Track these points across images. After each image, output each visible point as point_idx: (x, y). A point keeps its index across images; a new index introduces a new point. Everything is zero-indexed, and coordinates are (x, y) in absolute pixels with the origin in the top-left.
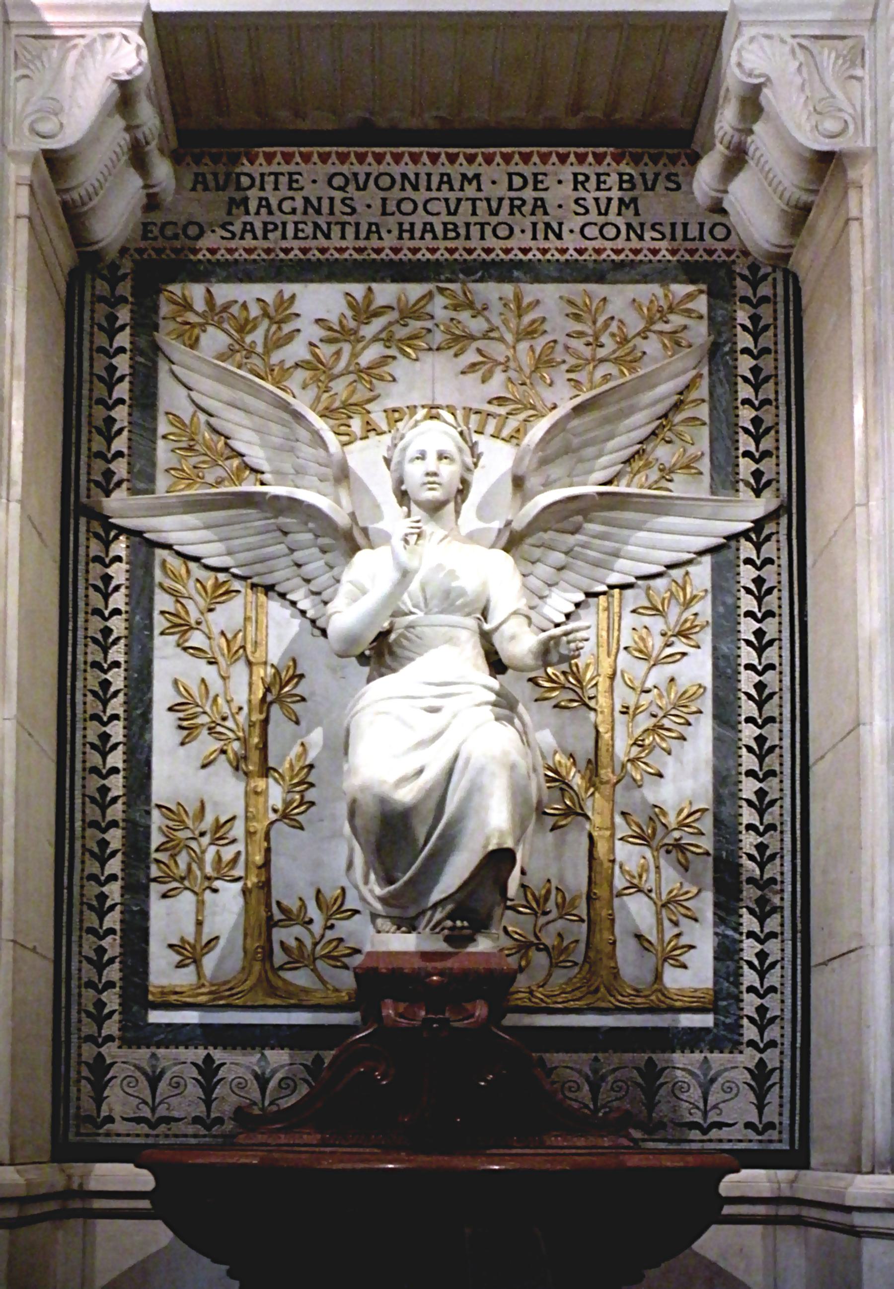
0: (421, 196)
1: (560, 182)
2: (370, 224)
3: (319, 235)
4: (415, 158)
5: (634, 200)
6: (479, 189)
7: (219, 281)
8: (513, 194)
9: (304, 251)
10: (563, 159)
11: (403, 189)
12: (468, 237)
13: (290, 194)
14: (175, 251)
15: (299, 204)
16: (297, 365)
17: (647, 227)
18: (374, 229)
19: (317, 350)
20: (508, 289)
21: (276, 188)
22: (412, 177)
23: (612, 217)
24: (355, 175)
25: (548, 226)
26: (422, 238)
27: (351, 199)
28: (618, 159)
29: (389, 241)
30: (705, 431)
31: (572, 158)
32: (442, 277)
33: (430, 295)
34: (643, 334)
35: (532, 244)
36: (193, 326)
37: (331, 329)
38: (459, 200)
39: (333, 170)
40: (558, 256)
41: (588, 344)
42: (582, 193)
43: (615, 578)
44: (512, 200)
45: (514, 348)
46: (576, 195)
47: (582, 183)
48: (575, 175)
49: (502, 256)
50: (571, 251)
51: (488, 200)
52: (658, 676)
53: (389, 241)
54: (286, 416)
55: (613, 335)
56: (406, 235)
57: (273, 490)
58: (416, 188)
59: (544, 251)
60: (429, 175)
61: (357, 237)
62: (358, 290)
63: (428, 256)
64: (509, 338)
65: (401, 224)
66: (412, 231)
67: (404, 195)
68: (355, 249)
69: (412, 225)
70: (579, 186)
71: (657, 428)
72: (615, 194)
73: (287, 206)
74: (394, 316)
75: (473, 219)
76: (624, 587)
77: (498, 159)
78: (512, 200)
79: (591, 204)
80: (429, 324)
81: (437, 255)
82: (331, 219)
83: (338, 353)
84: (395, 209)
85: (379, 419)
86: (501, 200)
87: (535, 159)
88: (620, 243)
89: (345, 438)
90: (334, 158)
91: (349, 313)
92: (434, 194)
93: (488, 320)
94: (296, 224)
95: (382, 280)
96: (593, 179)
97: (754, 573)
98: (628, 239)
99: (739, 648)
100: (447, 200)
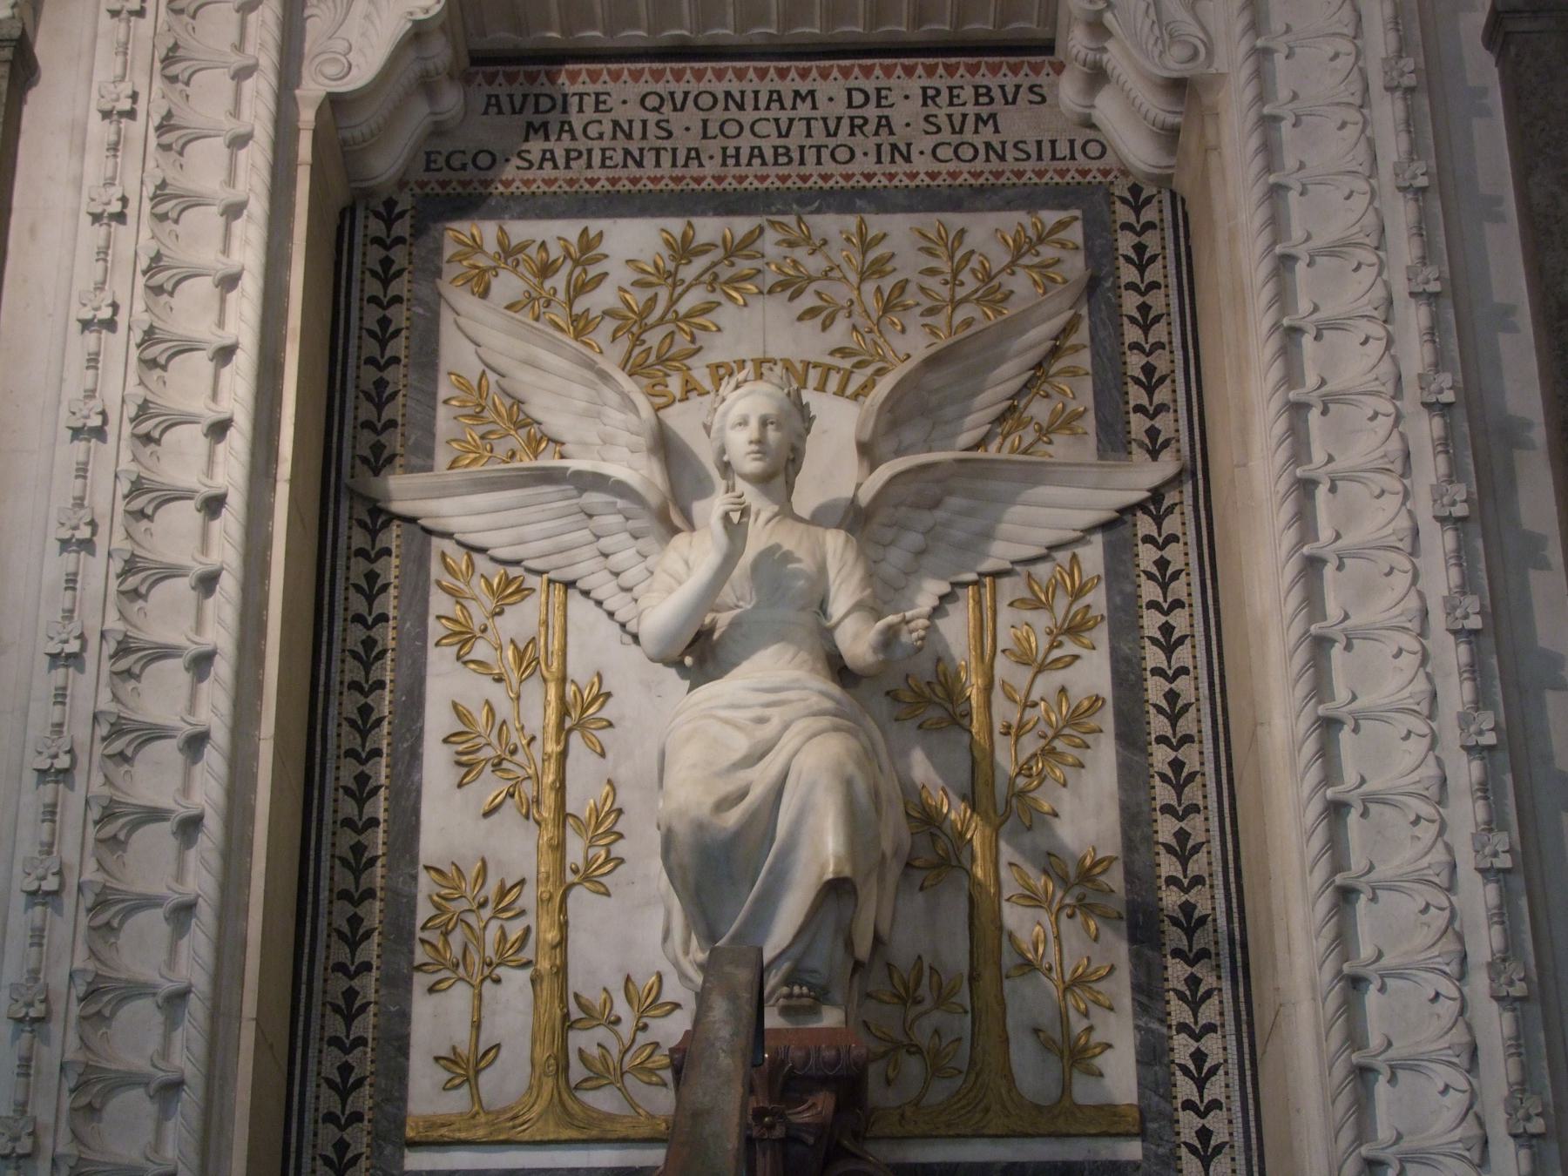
0: (747, 117)
1: (907, 97)
2: (689, 150)
3: (630, 162)
4: (740, 75)
5: (993, 116)
6: (814, 107)
7: (512, 218)
8: (853, 112)
9: (613, 181)
10: (909, 71)
11: (727, 108)
12: (802, 162)
13: (597, 116)
14: (464, 184)
15: (607, 128)
16: (606, 313)
17: (1009, 146)
18: (694, 155)
19: (628, 297)
20: (851, 222)
21: (581, 110)
22: (738, 97)
23: (968, 135)
24: (672, 94)
25: (894, 147)
26: (749, 164)
27: (667, 121)
28: (973, 70)
29: (711, 168)
31: (920, 71)
33: (761, 230)
34: (1011, 268)
35: (876, 168)
36: (483, 271)
37: (644, 271)
38: (791, 121)
39: (648, 89)
40: (906, 181)
41: (946, 283)
42: (932, 109)
43: (988, 565)
44: (852, 119)
45: (859, 288)
46: (926, 111)
47: (933, 98)
48: (924, 89)
50: (922, 176)
51: (825, 120)
52: (1046, 685)
53: (711, 168)
54: (590, 375)
55: (973, 271)
56: (731, 161)
57: (573, 464)
58: (741, 107)
59: (891, 177)
60: (756, 93)
61: (674, 165)
62: (676, 225)
63: (756, 184)
64: (853, 278)
65: (724, 149)
66: (737, 156)
67: (727, 115)
68: (671, 178)
69: (738, 149)
70: (929, 102)
71: (1029, 380)
72: (971, 109)
73: (593, 131)
74: (718, 254)
75: (809, 142)
76: (997, 575)
77: (835, 73)
78: (852, 119)
79: (943, 121)
80: (758, 264)
81: (767, 184)
82: (644, 144)
83: (653, 300)
85: (701, 375)
86: (839, 119)
87: (878, 72)
88: (979, 165)
89: (660, 401)
90: (647, 76)
91: (666, 253)
92: (763, 114)
93: (828, 258)
94: (603, 150)
95: (704, 214)
96: (945, 94)
97: (1155, 554)
98: (988, 160)
99: (1143, 648)
100: (777, 120)
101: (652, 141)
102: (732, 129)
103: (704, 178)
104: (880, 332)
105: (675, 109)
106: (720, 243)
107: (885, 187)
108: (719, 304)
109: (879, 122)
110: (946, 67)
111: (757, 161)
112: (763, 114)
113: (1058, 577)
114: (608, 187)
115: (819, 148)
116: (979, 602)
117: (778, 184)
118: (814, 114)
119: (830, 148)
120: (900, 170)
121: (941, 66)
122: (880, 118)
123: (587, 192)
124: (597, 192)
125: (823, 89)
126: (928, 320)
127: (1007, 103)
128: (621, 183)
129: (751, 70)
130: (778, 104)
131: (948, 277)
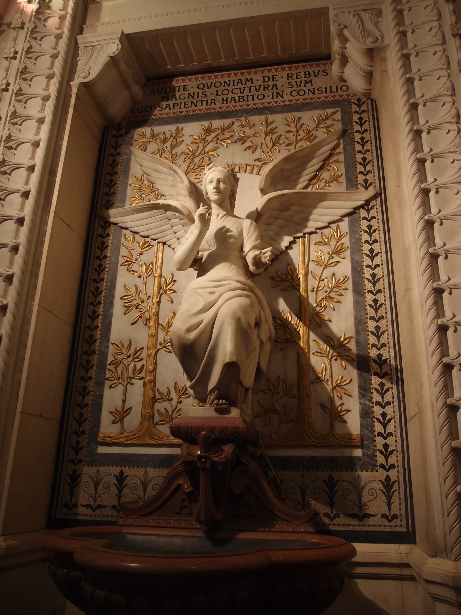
0: (230, 89)
1: (282, 77)
2: (212, 100)
4: (229, 76)
5: (311, 81)
6: (252, 83)
10: (283, 69)
11: (224, 86)
12: (248, 101)
17: (316, 90)
18: (213, 101)
20: (263, 118)
23: (302, 87)
26: (231, 102)
27: (205, 92)
28: (304, 67)
29: (218, 105)
30: (343, 165)
31: (287, 69)
32: (238, 116)
35: (272, 100)
38: (245, 88)
40: (281, 104)
41: (294, 135)
42: (290, 80)
44: (264, 86)
45: (265, 139)
46: (288, 81)
48: (288, 74)
49: (260, 106)
50: (287, 101)
51: (255, 87)
55: (303, 130)
59: (276, 102)
60: (234, 81)
61: (207, 105)
62: (206, 124)
63: (233, 108)
64: (263, 136)
65: (223, 99)
66: (227, 101)
67: (224, 88)
68: (206, 109)
69: (227, 98)
70: (290, 78)
72: (303, 79)
73: (182, 97)
74: (219, 131)
75: (250, 94)
77: (259, 72)
78: (264, 86)
79: (294, 84)
80: (232, 133)
84: (221, 93)
86: (260, 86)
87: (273, 70)
88: (306, 96)
91: (202, 132)
92: (236, 87)
95: (215, 119)
96: (295, 75)
98: (309, 94)
99: (363, 258)
100: (240, 88)
101: (201, 98)
102: (226, 92)
103: (216, 108)
104: (271, 153)
105: (208, 88)
106: (220, 128)
107: (275, 106)
108: (219, 147)
109: (273, 86)
110: (295, 67)
111: (233, 101)
112: (236, 87)
113: (332, 233)
114: (186, 113)
115: (253, 96)
116: (304, 244)
117: (240, 108)
118: (252, 85)
119: (257, 95)
120: (280, 100)
121: (293, 67)
122: (273, 85)
123: (179, 116)
124: (182, 115)
125: (255, 77)
126: (288, 148)
127: (315, 76)
128: (190, 112)
129: (233, 74)
130: (240, 83)
131: (295, 133)
